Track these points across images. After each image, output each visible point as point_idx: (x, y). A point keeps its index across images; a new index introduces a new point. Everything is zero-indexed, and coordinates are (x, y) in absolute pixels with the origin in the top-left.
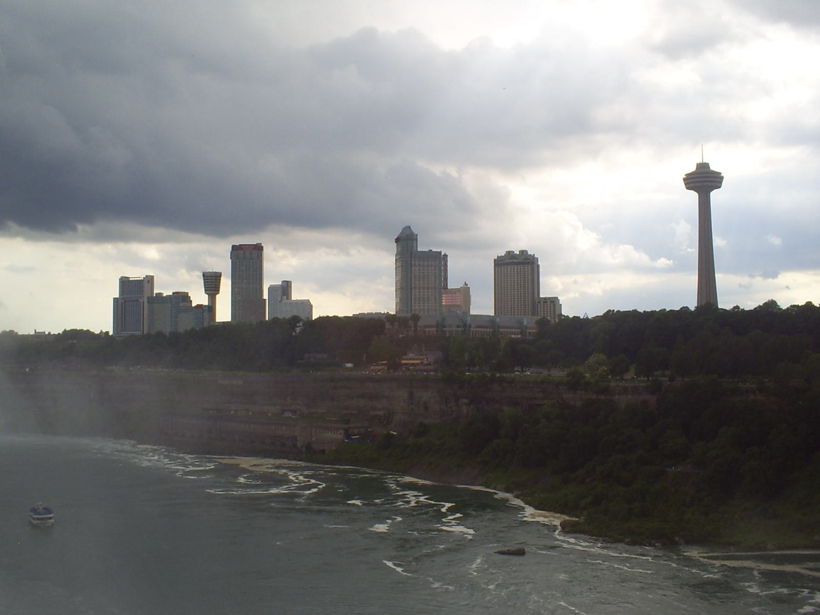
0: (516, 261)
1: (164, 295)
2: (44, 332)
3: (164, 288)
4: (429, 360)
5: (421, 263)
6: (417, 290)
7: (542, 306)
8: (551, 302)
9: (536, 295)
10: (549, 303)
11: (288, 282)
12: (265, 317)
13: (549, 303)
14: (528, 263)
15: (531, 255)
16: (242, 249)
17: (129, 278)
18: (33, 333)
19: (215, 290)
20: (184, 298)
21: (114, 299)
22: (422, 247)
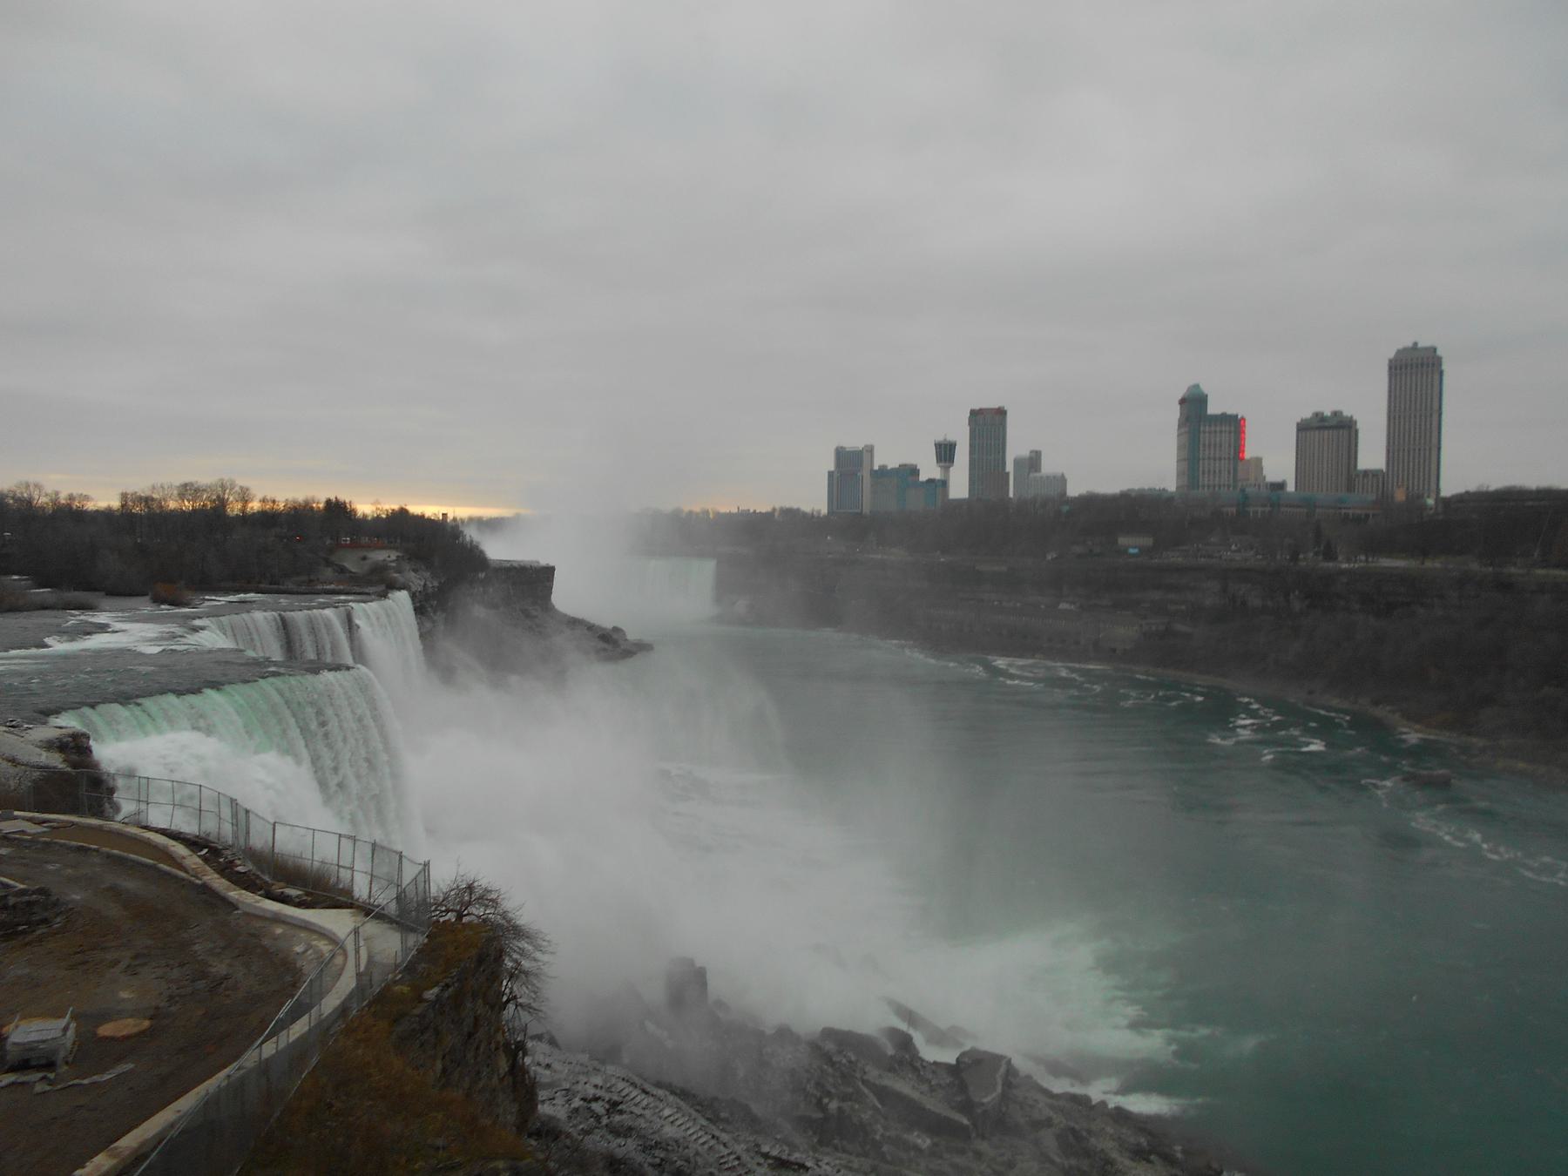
0: (1326, 424)
1: (889, 468)
2: (749, 510)
3: (887, 457)
4: (1239, 545)
8: (1373, 475)
9: (1352, 466)
10: (1370, 476)
12: (1008, 495)
13: (1370, 476)
15: (1347, 417)
16: (982, 413)
17: (845, 448)
18: (735, 510)
20: (914, 471)
21: (829, 472)
22: (1213, 409)
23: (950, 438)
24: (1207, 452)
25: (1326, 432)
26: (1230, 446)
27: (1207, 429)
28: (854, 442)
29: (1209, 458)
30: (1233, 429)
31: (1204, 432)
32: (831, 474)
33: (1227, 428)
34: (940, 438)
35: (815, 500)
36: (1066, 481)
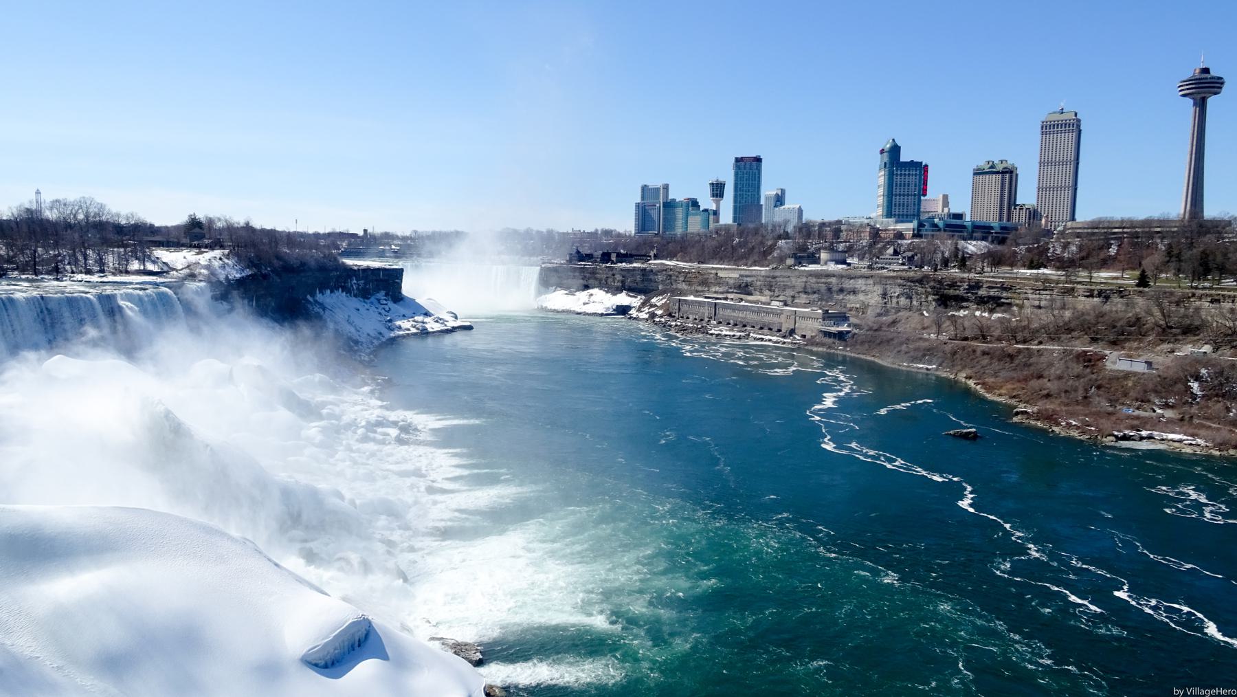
5: (903, 172)
6: (898, 197)
7: (1018, 212)
9: (1012, 203)
10: (1024, 210)
11: (782, 190)
14: (1007, 172)
19: (720, 197)
20: (695, 203)
22: (905, 157)
23: (721, 179)
24: (898, 190)
25: (994, 176)
26: (915, 186)
27: (899, 172)
28: (655, 182)
29: (900, 195)
30: (918, 172)
31: (897, 175)
32: (638, 205)
33: (914, 173)
34: (713, 180)
35: (626, 225)
36: (802, 211)
